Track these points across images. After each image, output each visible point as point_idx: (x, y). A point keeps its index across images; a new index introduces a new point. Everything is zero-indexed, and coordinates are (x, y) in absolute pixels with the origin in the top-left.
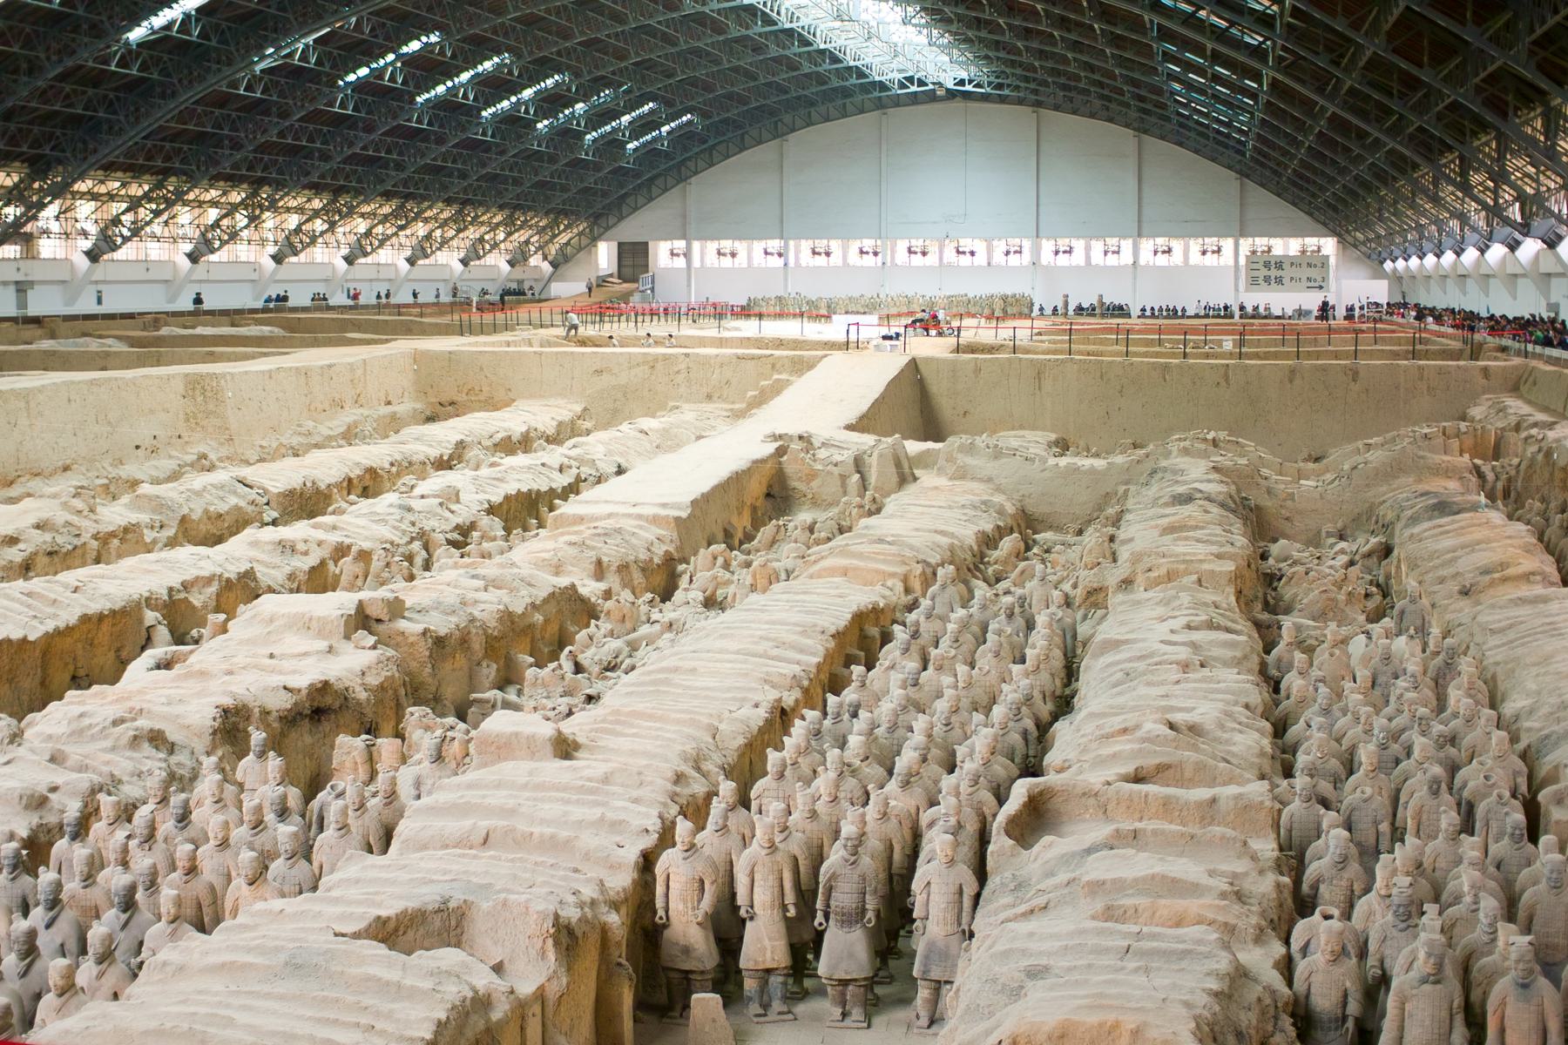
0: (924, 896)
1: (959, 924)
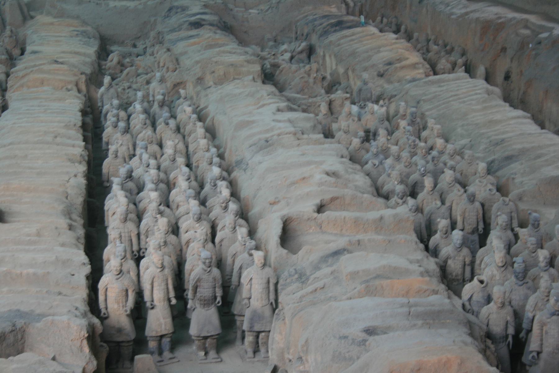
0: (249, 286)
1: (269, 300)
